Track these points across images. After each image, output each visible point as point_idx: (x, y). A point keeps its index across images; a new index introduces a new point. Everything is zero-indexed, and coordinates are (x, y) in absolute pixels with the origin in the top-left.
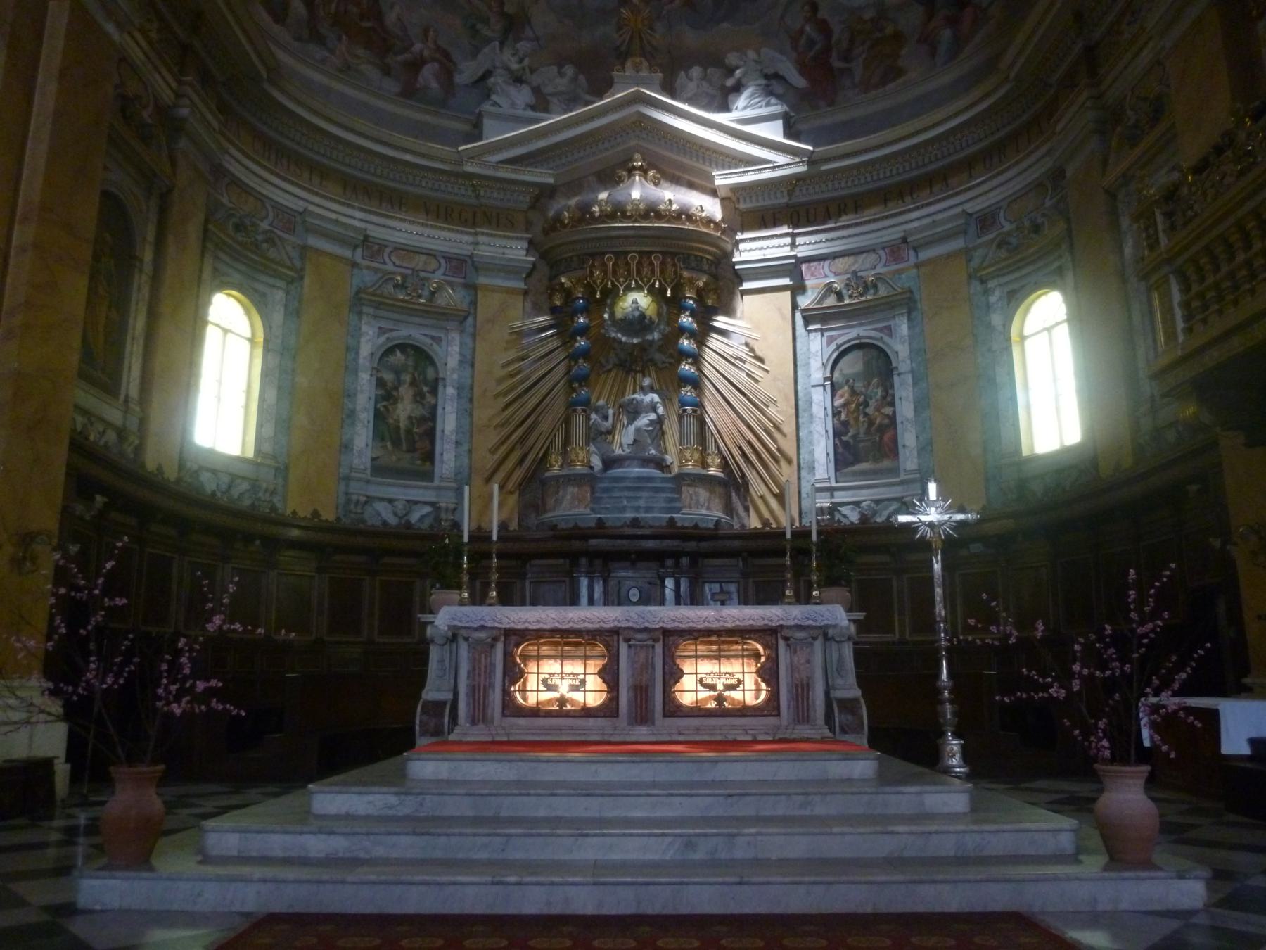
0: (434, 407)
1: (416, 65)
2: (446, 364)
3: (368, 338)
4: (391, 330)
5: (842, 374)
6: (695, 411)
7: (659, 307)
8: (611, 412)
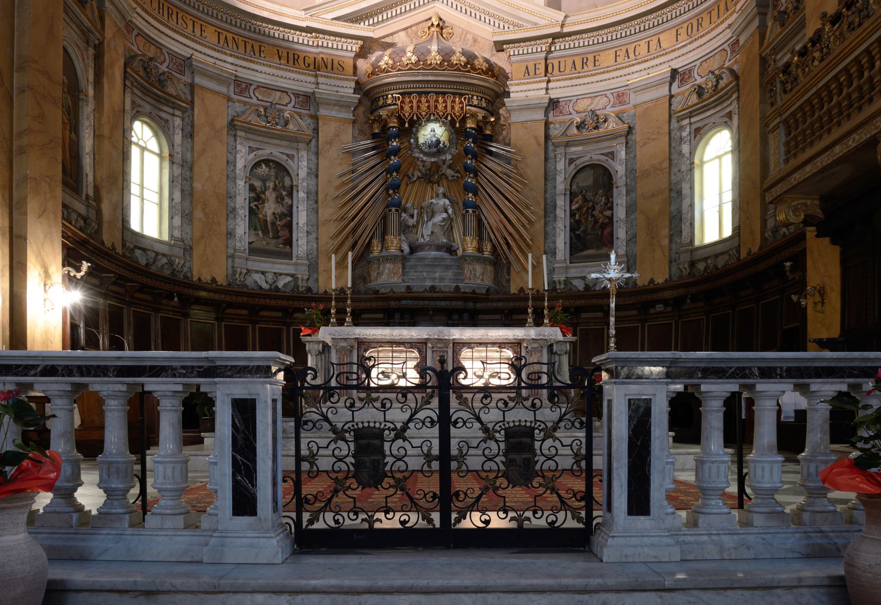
0: (291, 206)
2: (298, 175)
3: (242, 154)
4: (258, 149)
5: (577, 186)
6: (474, 212)
7: (451, 134)
8: (416, 211)
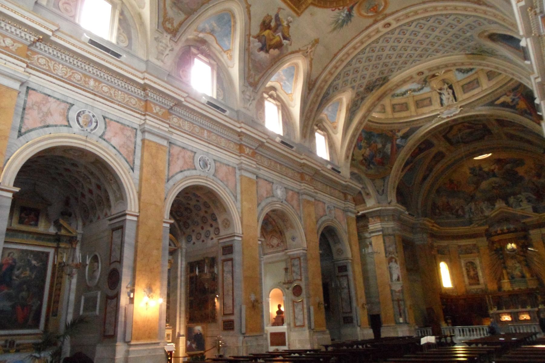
1: (457, 211)
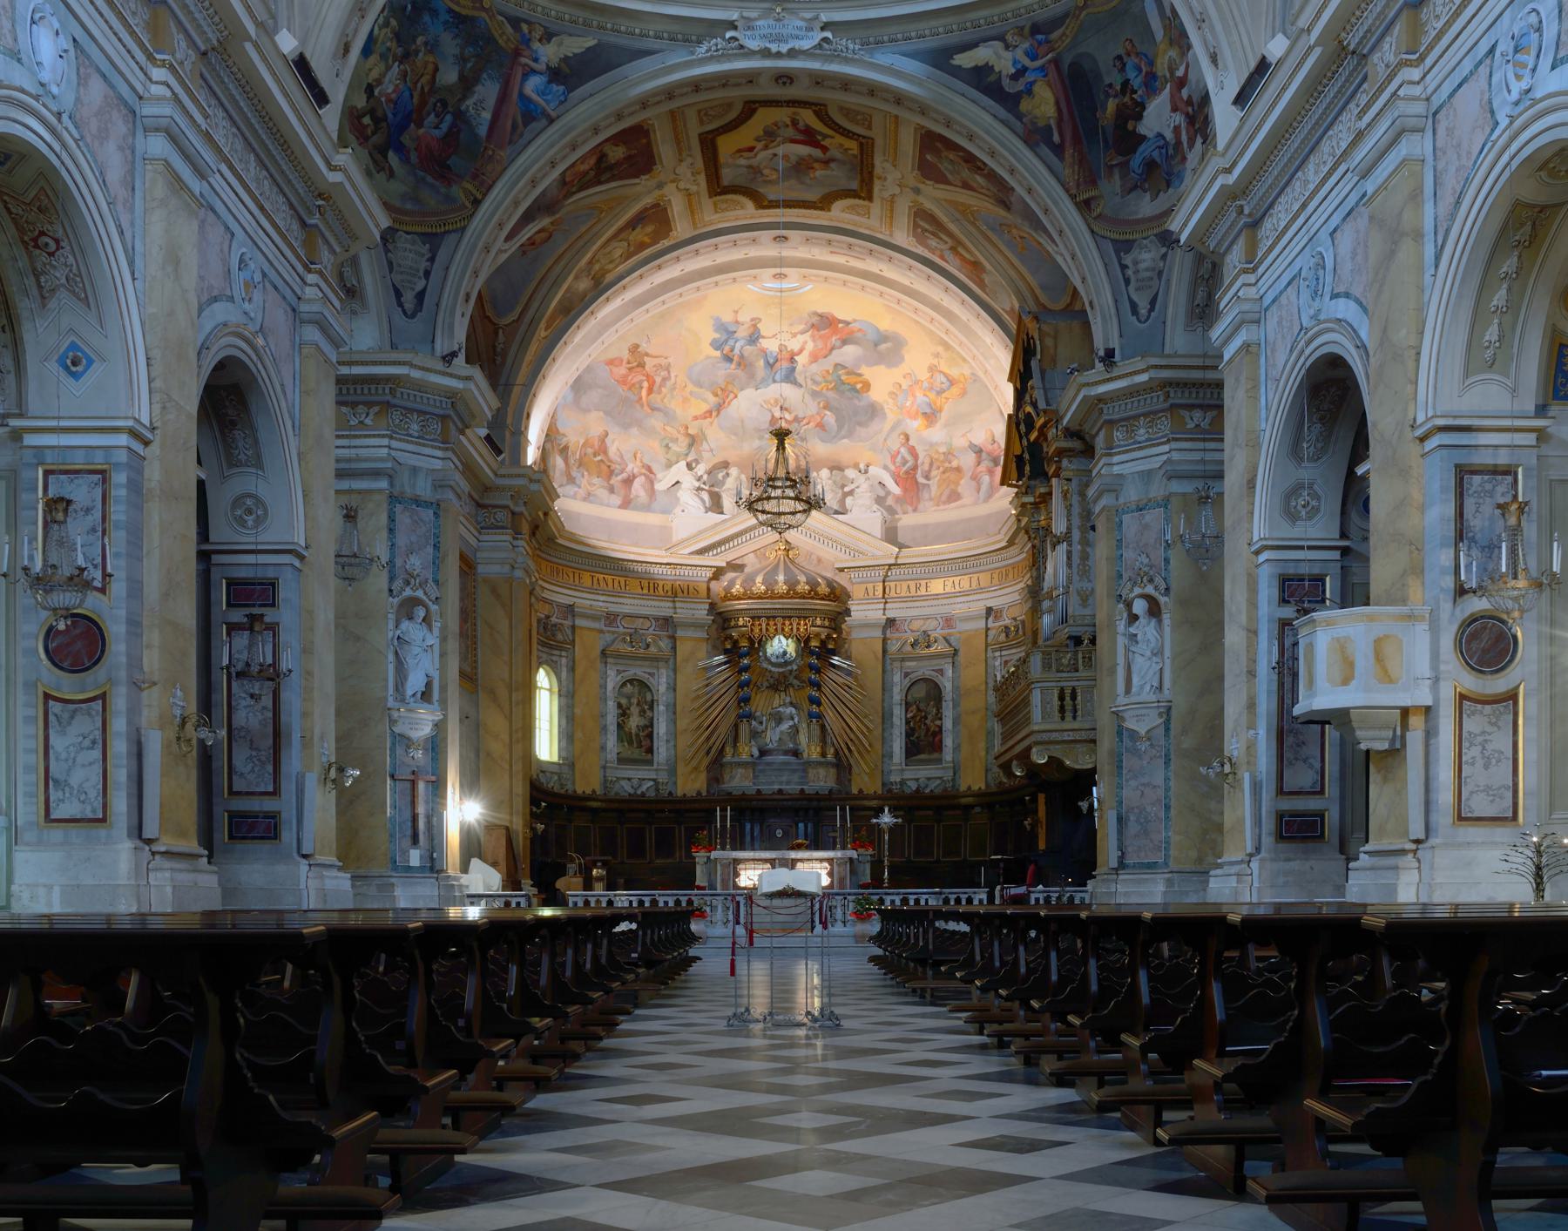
1: (629, 482)
